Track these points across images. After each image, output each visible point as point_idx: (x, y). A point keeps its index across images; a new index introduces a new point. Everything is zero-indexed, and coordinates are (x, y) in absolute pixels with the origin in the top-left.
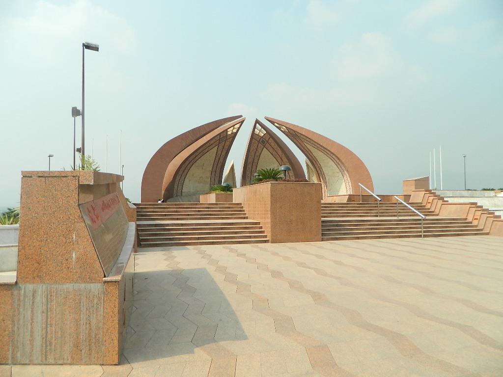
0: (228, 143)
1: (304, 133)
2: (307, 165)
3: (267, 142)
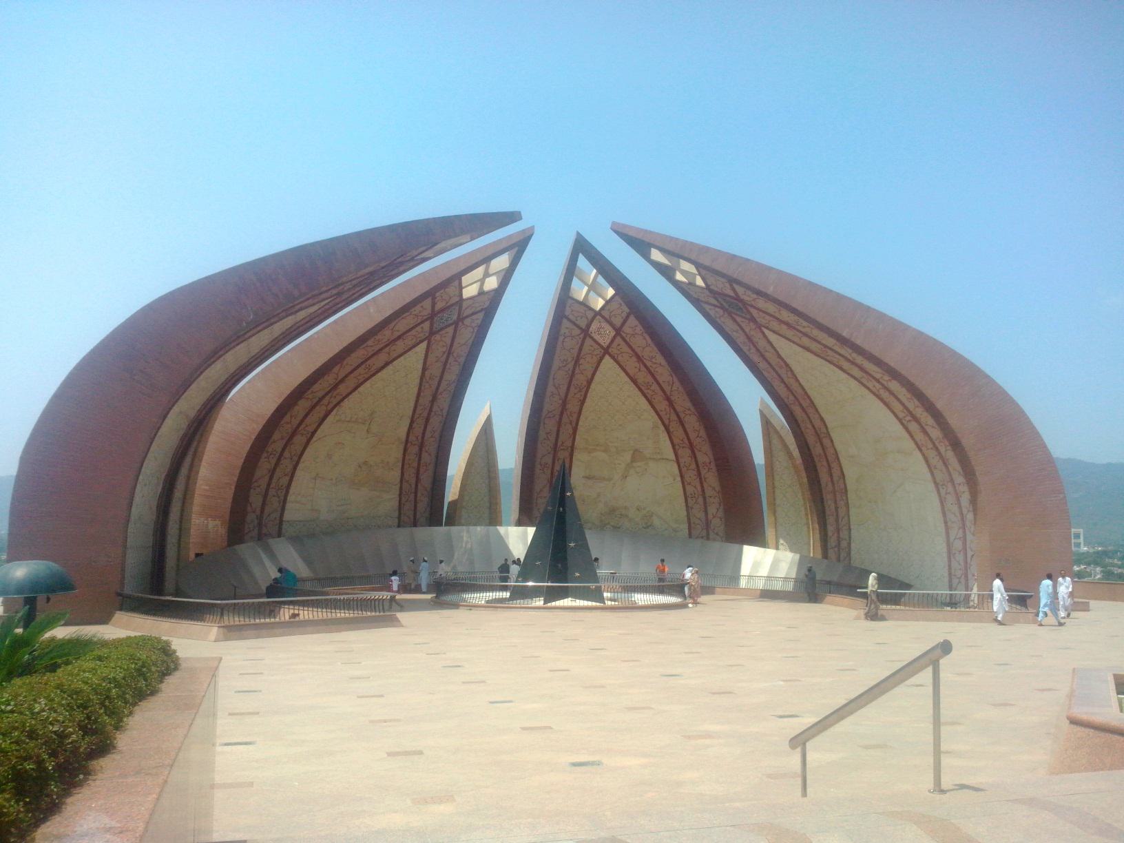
0: (466, 335)
1: (770, 291)
2: (767, 424)
3: (618, 331)
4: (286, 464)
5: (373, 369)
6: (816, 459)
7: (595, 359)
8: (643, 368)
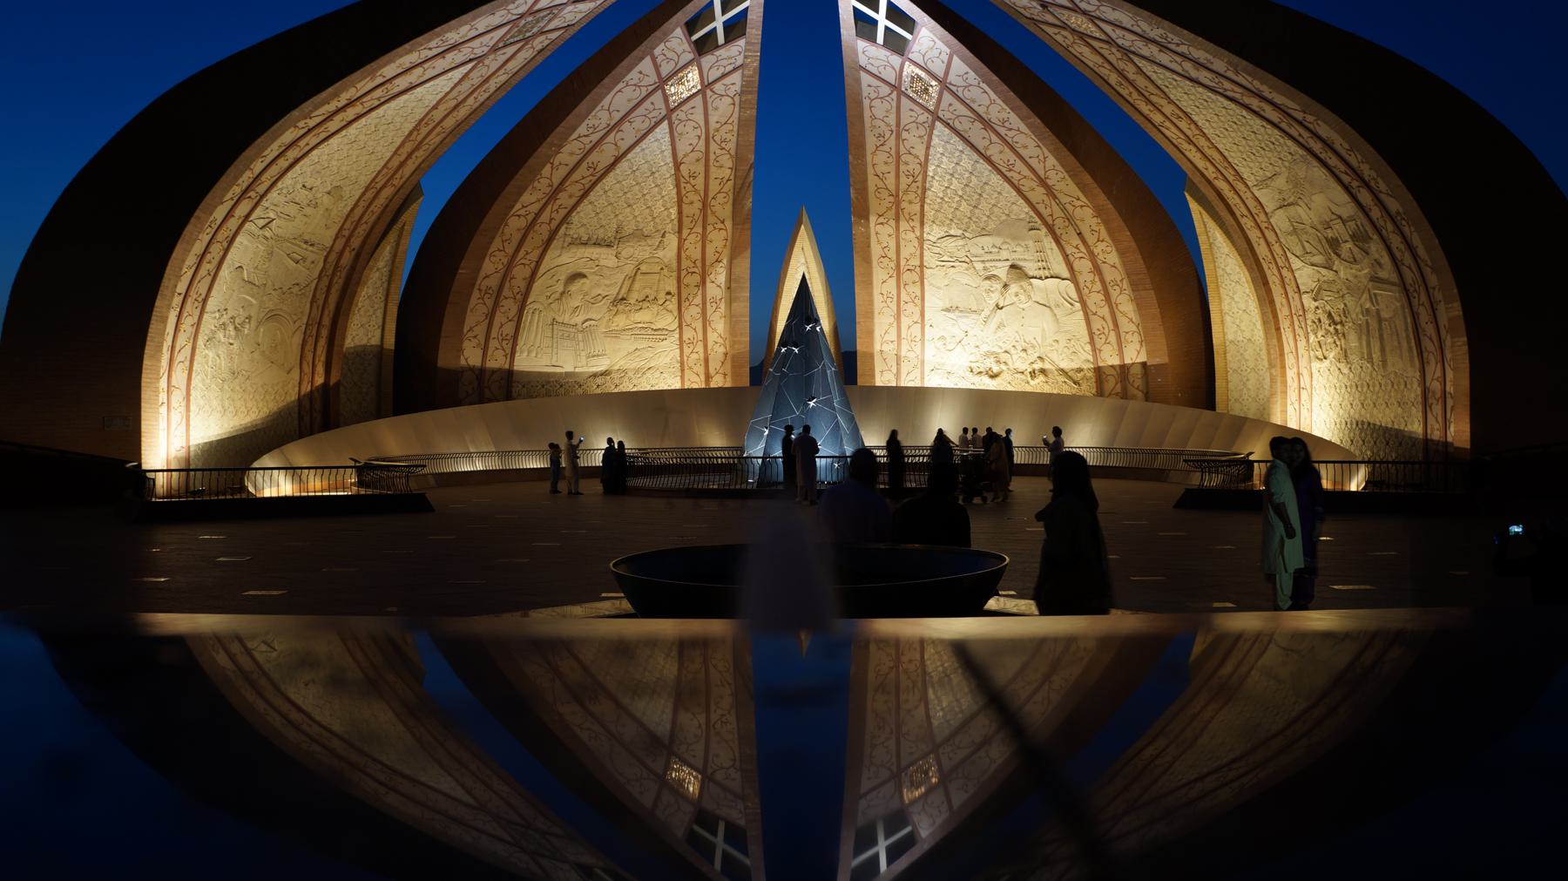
3: (944, 85)
4: (509, 307)
5: (601, 166)
6: (1265, 266)
7: (922, 131)
8: (994, 138)
